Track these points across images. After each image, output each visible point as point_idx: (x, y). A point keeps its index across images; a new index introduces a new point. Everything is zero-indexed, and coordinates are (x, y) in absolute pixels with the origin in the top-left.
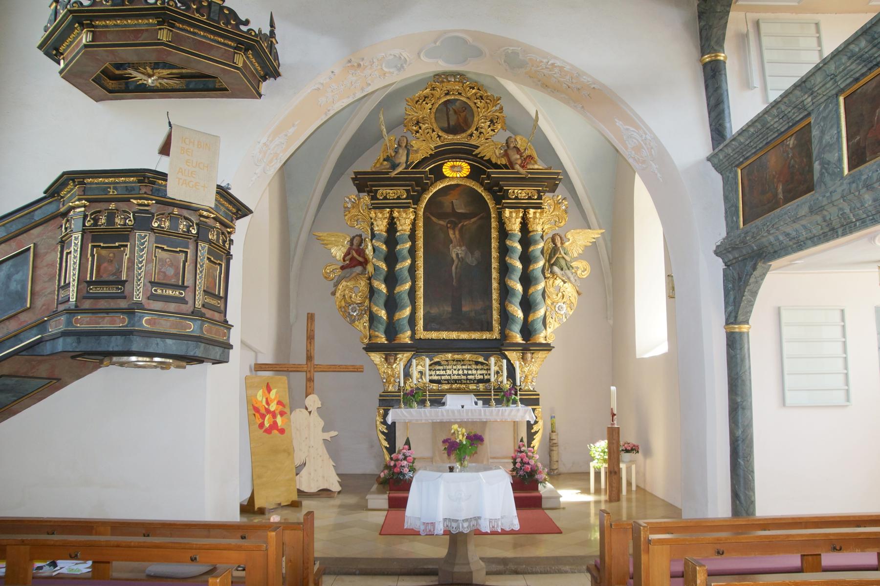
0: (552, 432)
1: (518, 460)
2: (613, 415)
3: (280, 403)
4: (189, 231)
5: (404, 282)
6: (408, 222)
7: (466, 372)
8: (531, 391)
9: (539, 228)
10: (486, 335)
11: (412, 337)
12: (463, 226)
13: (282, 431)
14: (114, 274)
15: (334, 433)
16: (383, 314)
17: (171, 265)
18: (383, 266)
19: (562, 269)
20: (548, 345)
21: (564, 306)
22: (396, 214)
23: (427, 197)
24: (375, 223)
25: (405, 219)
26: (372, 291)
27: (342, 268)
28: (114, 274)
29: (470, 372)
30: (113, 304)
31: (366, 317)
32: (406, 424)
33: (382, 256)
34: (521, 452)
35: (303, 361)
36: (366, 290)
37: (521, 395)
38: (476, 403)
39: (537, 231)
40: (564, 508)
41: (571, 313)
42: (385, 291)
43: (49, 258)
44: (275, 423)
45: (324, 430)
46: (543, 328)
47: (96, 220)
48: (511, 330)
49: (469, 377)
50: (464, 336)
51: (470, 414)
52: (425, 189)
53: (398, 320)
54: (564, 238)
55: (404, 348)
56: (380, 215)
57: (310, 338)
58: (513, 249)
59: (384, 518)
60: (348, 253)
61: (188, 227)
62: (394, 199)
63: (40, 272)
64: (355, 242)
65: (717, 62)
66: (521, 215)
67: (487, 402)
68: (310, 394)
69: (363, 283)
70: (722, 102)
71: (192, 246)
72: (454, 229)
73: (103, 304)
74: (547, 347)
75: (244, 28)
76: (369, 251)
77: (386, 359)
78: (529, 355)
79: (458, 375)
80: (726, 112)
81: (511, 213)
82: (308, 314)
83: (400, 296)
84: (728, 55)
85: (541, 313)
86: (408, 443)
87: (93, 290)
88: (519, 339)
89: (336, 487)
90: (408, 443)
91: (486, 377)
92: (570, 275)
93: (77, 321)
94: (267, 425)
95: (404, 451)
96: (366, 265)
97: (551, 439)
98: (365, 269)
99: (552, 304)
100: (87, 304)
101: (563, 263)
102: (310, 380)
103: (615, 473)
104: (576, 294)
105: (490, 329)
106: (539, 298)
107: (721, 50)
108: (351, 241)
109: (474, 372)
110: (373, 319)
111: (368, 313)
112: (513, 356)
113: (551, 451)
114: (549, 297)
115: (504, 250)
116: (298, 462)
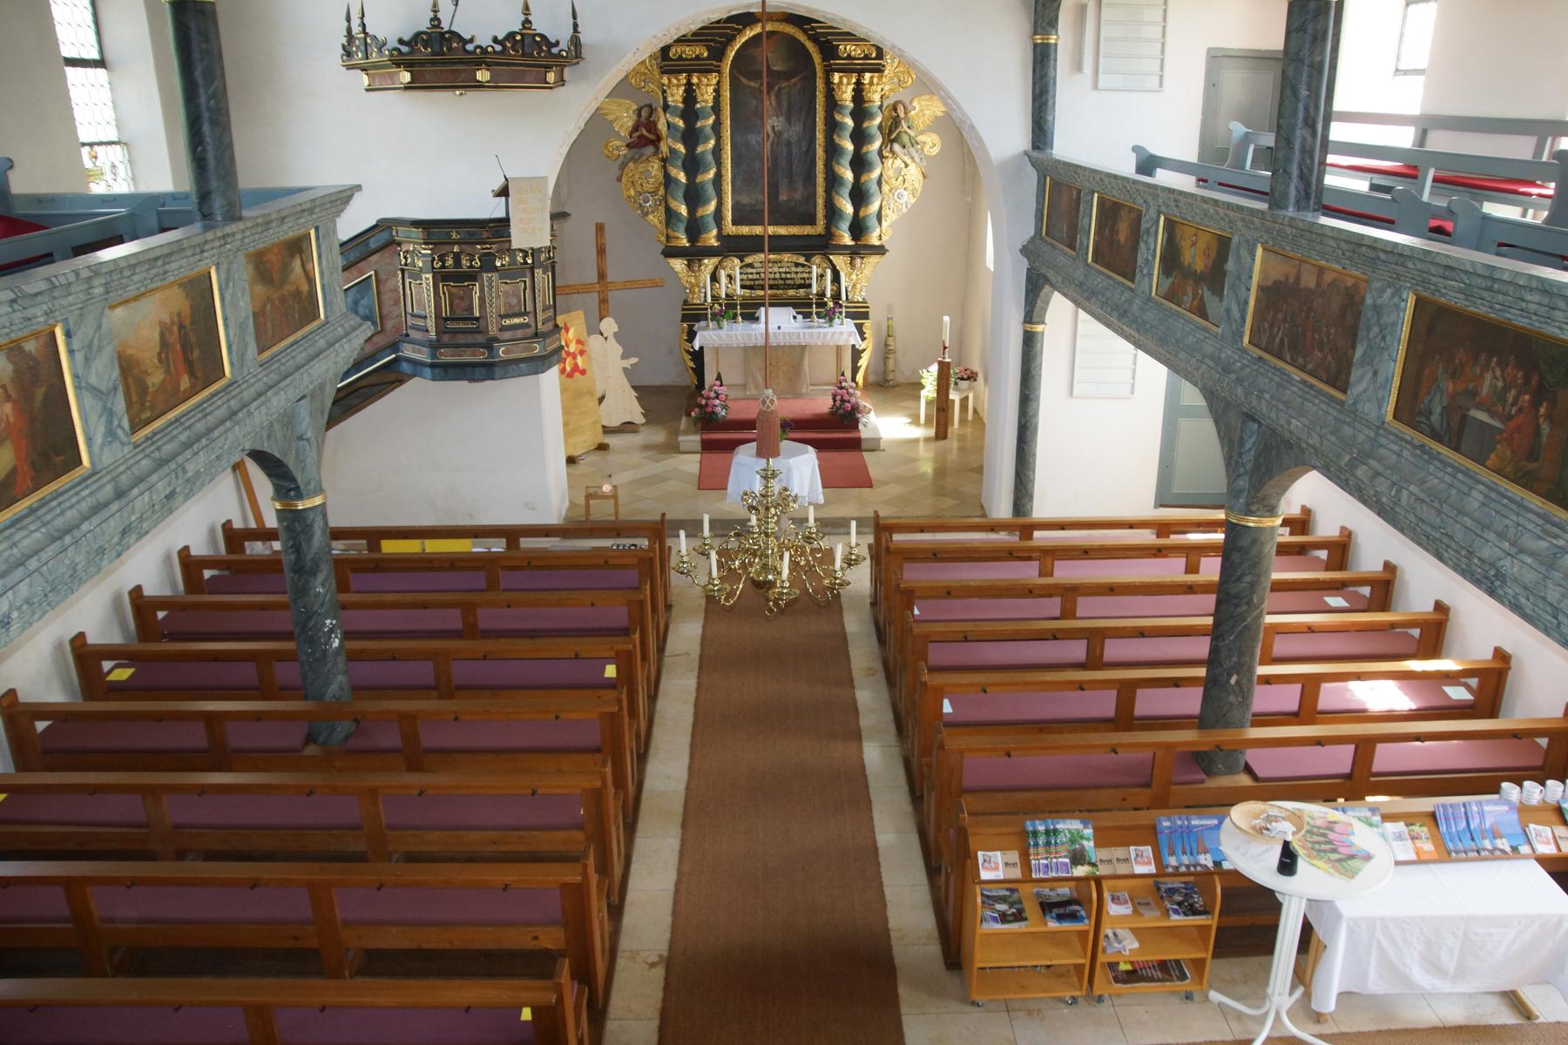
1: (838, 398)
2: (945, 348)
3: (579, 342)
4: (526, 263)
5: (706, 171)
6: (710, 89)
7: (783, 276)
8: (859, 302)
9: (876, 97)
10: (807, 230)
11: (720, 237)
12: (780, 89)
13: (583, 372)
14: (466, 310)
15: (634, 360)
16: (683, 210)
17: (514, 295)
18: (681, 148)
19: (904, 147)
20: (882, 247)
21: (905, 193)
22: (695, 80)
23: (731, 54)
24: (668, 91)
25: (708, 85)
26: (668, 181)
27: (629, 146)
29: (788, 276)
30: (470, 339)
31: (662, 209)
32: (717, 350)
33: (679, 135)
34: (841, 388)
35: (595, 279)
36: (661, 176)
37: (846, 307)
38: (795, 318)
41: (913, 201)
43: (390, 284)
45: (624, 357)
46: (877, 224)
47: (444, 262)
49: (788, 282)
50: (782, 231)
52: (731, 39)
53: (702, 217)
54: (909, 108)
55: (710, 252)
56: (675, 81)
57: (601, 251)
60: (636, 128)
61: (524, 258)
62: (692, 59)
63: (385, 297)
64: (644, 113)
65: (1048, 45)
66: (854, 80)
67: (807, 316)
68: (605, 317)
69: (656, 166)
71: (528, 274)
73: (461, 339)
74: (880, 250)
76: (662, 126)
77: (689, 266)
79: (775, 279)
80: (1050, 103)
81: (841, 78)
84: (1062, 38)
85: (874, 207)
86: (719, 378)
87: (450, 325)
88: (847, 240)
90: (719, 378)
91: (807, 282)
92: (914, 154)
93: (441, 354)
94: (568, 369)
95: (716, 388)
96: (659, 142)
97: (886, 345)
98: (657, 148)
99: (890, 191)
100: (446, 338)
101: (905, 139)
102: (603, 301)
103: (943, 410)
104: (921, 178)
105: (812, 222)
106: (874, 187)
107: (1054, 32)
109: (793, 276)
110: (670, 215)
111: (663, 204)
112: (840, 261)
113: (886, 358)
114: (886, 182)
115: (833, 127)
116: (599, 395)
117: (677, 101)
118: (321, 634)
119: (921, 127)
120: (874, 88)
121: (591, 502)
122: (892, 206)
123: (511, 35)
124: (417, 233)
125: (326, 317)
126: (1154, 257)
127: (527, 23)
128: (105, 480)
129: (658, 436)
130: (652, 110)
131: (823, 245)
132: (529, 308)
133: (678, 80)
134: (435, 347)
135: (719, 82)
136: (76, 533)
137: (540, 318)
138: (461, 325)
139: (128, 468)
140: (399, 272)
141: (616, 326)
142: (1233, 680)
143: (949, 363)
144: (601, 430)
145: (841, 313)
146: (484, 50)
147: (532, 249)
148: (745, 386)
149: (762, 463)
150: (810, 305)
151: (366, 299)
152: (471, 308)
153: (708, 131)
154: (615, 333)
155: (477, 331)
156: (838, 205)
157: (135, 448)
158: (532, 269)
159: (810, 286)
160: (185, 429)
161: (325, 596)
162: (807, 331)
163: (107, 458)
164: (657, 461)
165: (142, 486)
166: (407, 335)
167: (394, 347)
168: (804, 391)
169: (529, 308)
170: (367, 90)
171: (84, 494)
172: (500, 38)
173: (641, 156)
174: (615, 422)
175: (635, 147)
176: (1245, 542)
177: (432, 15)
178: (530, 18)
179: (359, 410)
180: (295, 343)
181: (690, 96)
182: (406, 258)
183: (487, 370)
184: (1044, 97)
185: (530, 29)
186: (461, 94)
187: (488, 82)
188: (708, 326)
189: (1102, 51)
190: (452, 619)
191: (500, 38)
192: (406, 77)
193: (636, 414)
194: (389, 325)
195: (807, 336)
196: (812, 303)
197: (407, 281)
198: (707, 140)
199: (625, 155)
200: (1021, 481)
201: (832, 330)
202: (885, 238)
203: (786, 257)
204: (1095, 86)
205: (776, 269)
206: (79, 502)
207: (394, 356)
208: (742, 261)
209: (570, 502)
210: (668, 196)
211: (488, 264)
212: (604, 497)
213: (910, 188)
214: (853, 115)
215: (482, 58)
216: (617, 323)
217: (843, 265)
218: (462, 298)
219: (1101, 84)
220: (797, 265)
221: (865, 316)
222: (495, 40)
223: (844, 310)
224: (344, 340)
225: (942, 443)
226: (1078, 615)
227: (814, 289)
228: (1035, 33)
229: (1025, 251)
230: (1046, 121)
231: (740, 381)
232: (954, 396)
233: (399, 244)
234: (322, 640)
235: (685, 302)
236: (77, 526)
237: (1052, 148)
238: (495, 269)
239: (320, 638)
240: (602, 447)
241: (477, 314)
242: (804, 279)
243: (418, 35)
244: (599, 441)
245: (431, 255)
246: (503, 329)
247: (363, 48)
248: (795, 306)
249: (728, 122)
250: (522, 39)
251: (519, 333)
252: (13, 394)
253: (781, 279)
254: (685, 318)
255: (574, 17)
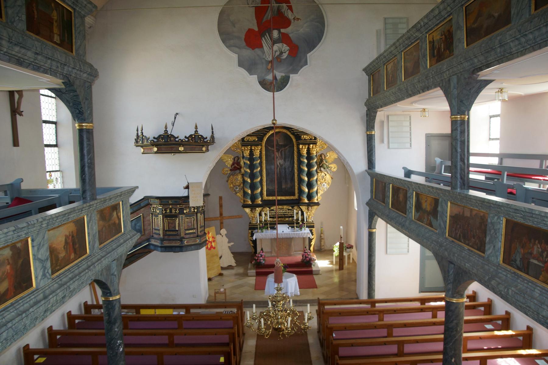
0: (321, 233)
1: (304, 256)
2: (341, 237)
3: (213, 237)
4: (194, 211)
5: (257, 178)
6: (258, 151)
7: (284, 213)
9: (315, 152)
10: (292, 198)
11: (262, 200)
12: (282, 150)
13: (214, 248)
14: (173, 228)
15: (232, 244)
16: (249, 192)
19: (325, 169)
20: (318, 203)
21: (326, 184)
22: (253, 148)
23: (265, 139)
25: (258, 150)
26: (244, 182)
27: (231, 170)
28: (173, 228)
29: (286, 213)
31: (242, 191)
32: (261, 240)
33: (248, 167)
34: (305, 253)
36: (241, 180)
37: (306, 224)
38: (288, 228)
39: (314, 154)
40: (321, 274)
41: (328, 187)
42: (249, 182)
43: (148, 218)
44: (212, 246)
45: (229, 242)
46: (316, 195)
47: (166, 211)
48: (303, 197)
49: (286, 215)
50: (283, 198)
51: (286, 235)
52: (265, 135)
53: (256, 194)
54: (326, 155)
55: (259, 206)
56: (246, 149)
57: (221, 206)
58: (303, 162)
59: (255, 281)
60: (233, 164)
61: (194, 210)
62: (252, 141)
64: (236, 159)
65: (372, 135)
66: (307, 147)
67: (293, 227)
69: (240, 177)
70: (372, 150)
71: (195, 215)
72: (278, 152)
73: (171, 238)
74: (317, 204)
75: (205, 140)
76: (242, 163)
77: (251, 211)
78: (310, 208)
79: (281, 215)
80: (373, 154)
81: (302, 146)
82: (219, 197)
83: (256, 184)
84: (376, 132)
85: (315, 189)
86: (262, 250)
87: (168, 233)
88: (306, 201)
89: (234, 264)
90: (262, 250)
91: (293, 215)
92: (328, 171)
93: (164, 243)
94: (209, 247)
95: (261, 253)
97: (321, 237)
98: (240, 170)
99: (320, 184)
100: (166, 237)
101: (325, 166)
102: (222, 223)
103: (342, 259)
104: (331, 179)
105: (294, 194)
106: (315, 183)
108: (234, 159)
109: (288, 213)
110: (245, 193)
112: (304, 208)
113: (321, 241)
115: (300, 163)
116: (220, 256)
117: (247, 155)
118: (116, 346)
119: (330, 162)
120: (314, 149)
121: (216, 295)
122: (321, 188)
123: (191, 136)
124: (157, 201)
125: (124, 231)
126: (413, 206)
127: (196, 131)
128: (40, 292)
129: (241, 270)
130: (239, 158)
131: (298, 203)
132: (195, 227)
133: (248, 148)
134: (162, 240)
135: (261, 148)
136: (28, 313)
137: (199, 230)
138: (172, 233)
139: (49, 288)
140: (151, 214)
141: (226, 232)
142: (453, 360)
143: (343, 243)
144: (220, 268)
145: (304, 226)
146: (182, 141)
147: (197, 207)
148: (271, 252)
149: (276, 285)
150: (293, 223)
151: (139, 224)
152: (175, 227)
153: (258, 165)
154: (226, 234)
155: (177, 235)
156: (302, 189)
157: (53, 280)
158: (197, 213)
159: (293, 217)
160: (71, 273)
161: (118, 332)
162: (292, 232)
163: (42, 284)
164: (240, 280)
165: (54, 294)
166: (153, 236)
167: (148, 240)
168: (292, 254)
169: (195, 227)
170: (143, 153)
171: (32, 297)
172: (187, 136)
173: (235, 174)
174: (225, 265)
175: (233, 170)
176: (453, 308)
177: (165, 129)
178: (197, 130)
179: (135, 262)
180: (113, 241)
181: (251, 153)
182: (153, 209)
183: (180, 249)
184: (371, 152)
185: (197, 133)
186: (174, 155)
187: (183, 151)
188: (258, 231)
189: (390, 136)
190: (165, 340)
191: (187, 136)
192: (155, 149)
193: (233, 262)
194: (147, 232)
195: (293, 235)
196: (294, 223)
197: (153, 217)
198: (257, 168)
199: (229, 173)
200: (370, 285)
201: (302, 232)
202: (319, 200)
203: (285, 207)
204: (389, 148)
205: (281, 211)
206: (30, 301)
207: (148, 243)
208: (270, 209)
209: (209, 295)
210: (244, 187)
211: (181, 212)
212: (221, 293)
213: (327, 182)
214: (307, 158)
215: (181, 143)
216: (226, 231)
217: (305, 210)
218: (172, 224)
219: (390, 147)
220: (289, 210)
221: (313, 227)
222: (186, 137)
223: (305, 225)
224: (130, 240)
225: (341, 271)
226: (394, 335)
227: (295, 218)
228: (367, 131)
229: (368, 204)
230: (372, 160)
231: (269, 250)
232: (345, 254)
233: (151, 205)
234: (116, 348)
235: (250, 223)
236: (28, 310)
237: (375, 169)
238: (184, 213)
239: (115, 348)
240: (221, 275)
241: (177, 229)
242: (291, 214)
243: (160, 136)
244: (220, 272)
245: (162, 209)
246: (186, 234)
247: (142, 140)
248: (288, 224)
249: (264, 162)
250: (195, 137)
251: (192, 236)
252: (11, 261)
253: (283, 215)
254: (250, 229)
255: (212, 129)
